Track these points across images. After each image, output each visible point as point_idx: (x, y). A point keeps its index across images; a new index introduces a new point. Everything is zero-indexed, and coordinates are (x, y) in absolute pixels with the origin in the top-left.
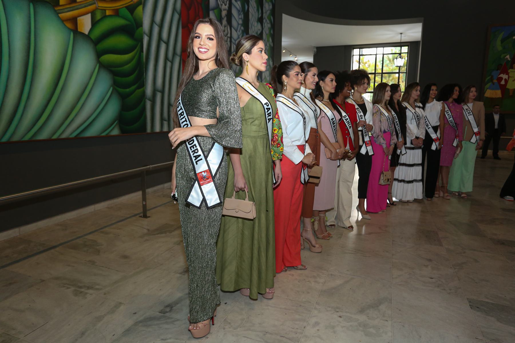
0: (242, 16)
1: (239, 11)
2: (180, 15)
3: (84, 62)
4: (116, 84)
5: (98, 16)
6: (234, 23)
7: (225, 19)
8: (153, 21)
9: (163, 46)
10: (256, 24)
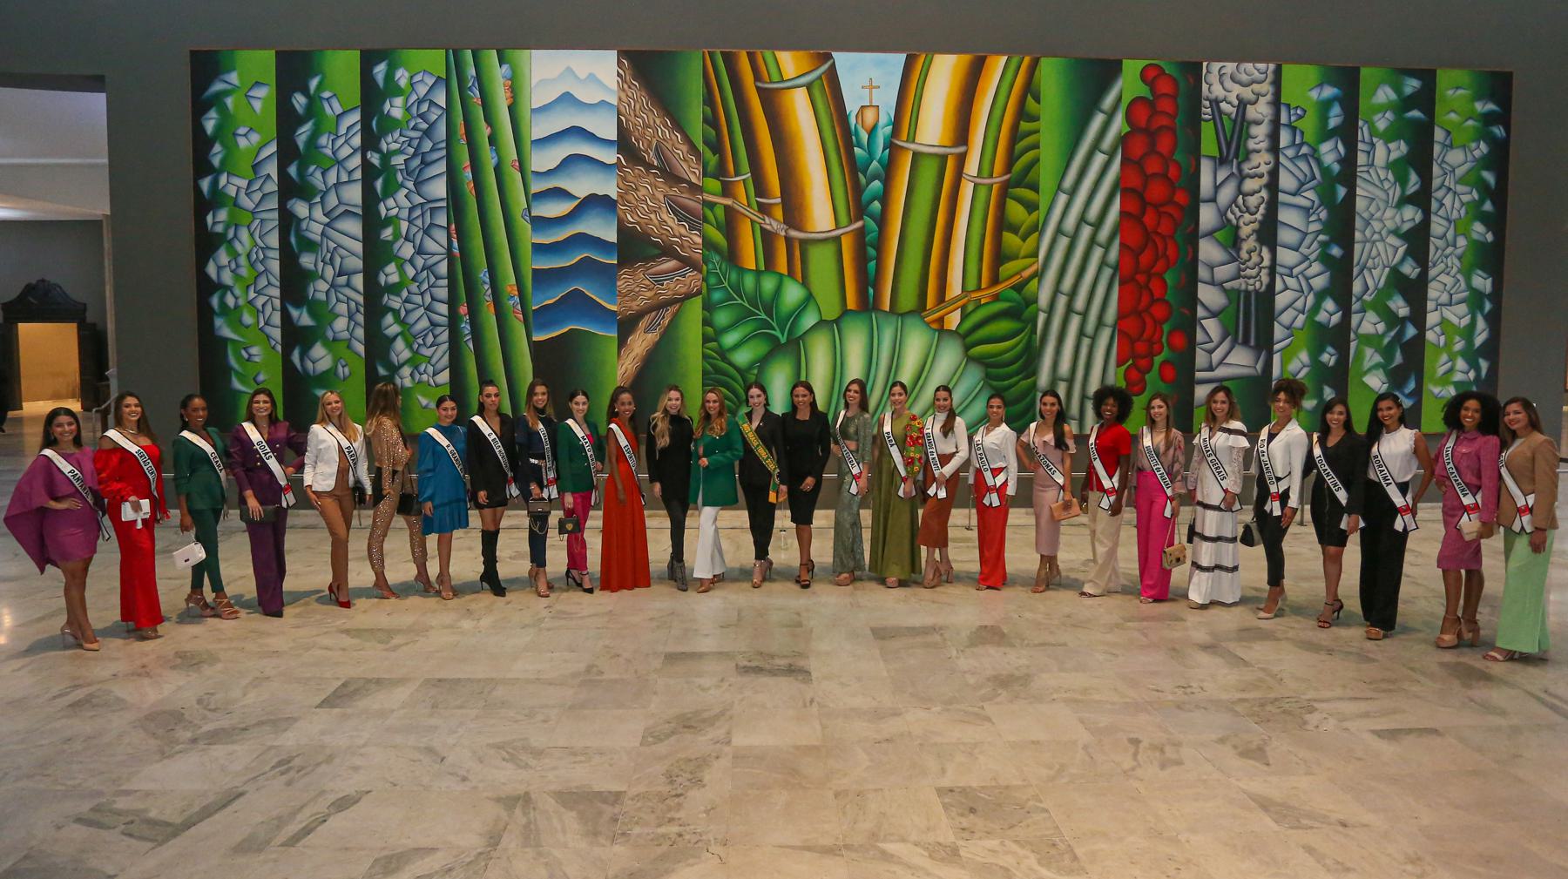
0: (1323, 215)
1: (1307, 211)
2: (1117, 268)
3: (949, 358)
4: (988, 377)
5: (970, 308)
6: (1285, 236)
7: (1253, 237)
8: (1056, 291)
9: (1075, 321)
10: (1389, 213)
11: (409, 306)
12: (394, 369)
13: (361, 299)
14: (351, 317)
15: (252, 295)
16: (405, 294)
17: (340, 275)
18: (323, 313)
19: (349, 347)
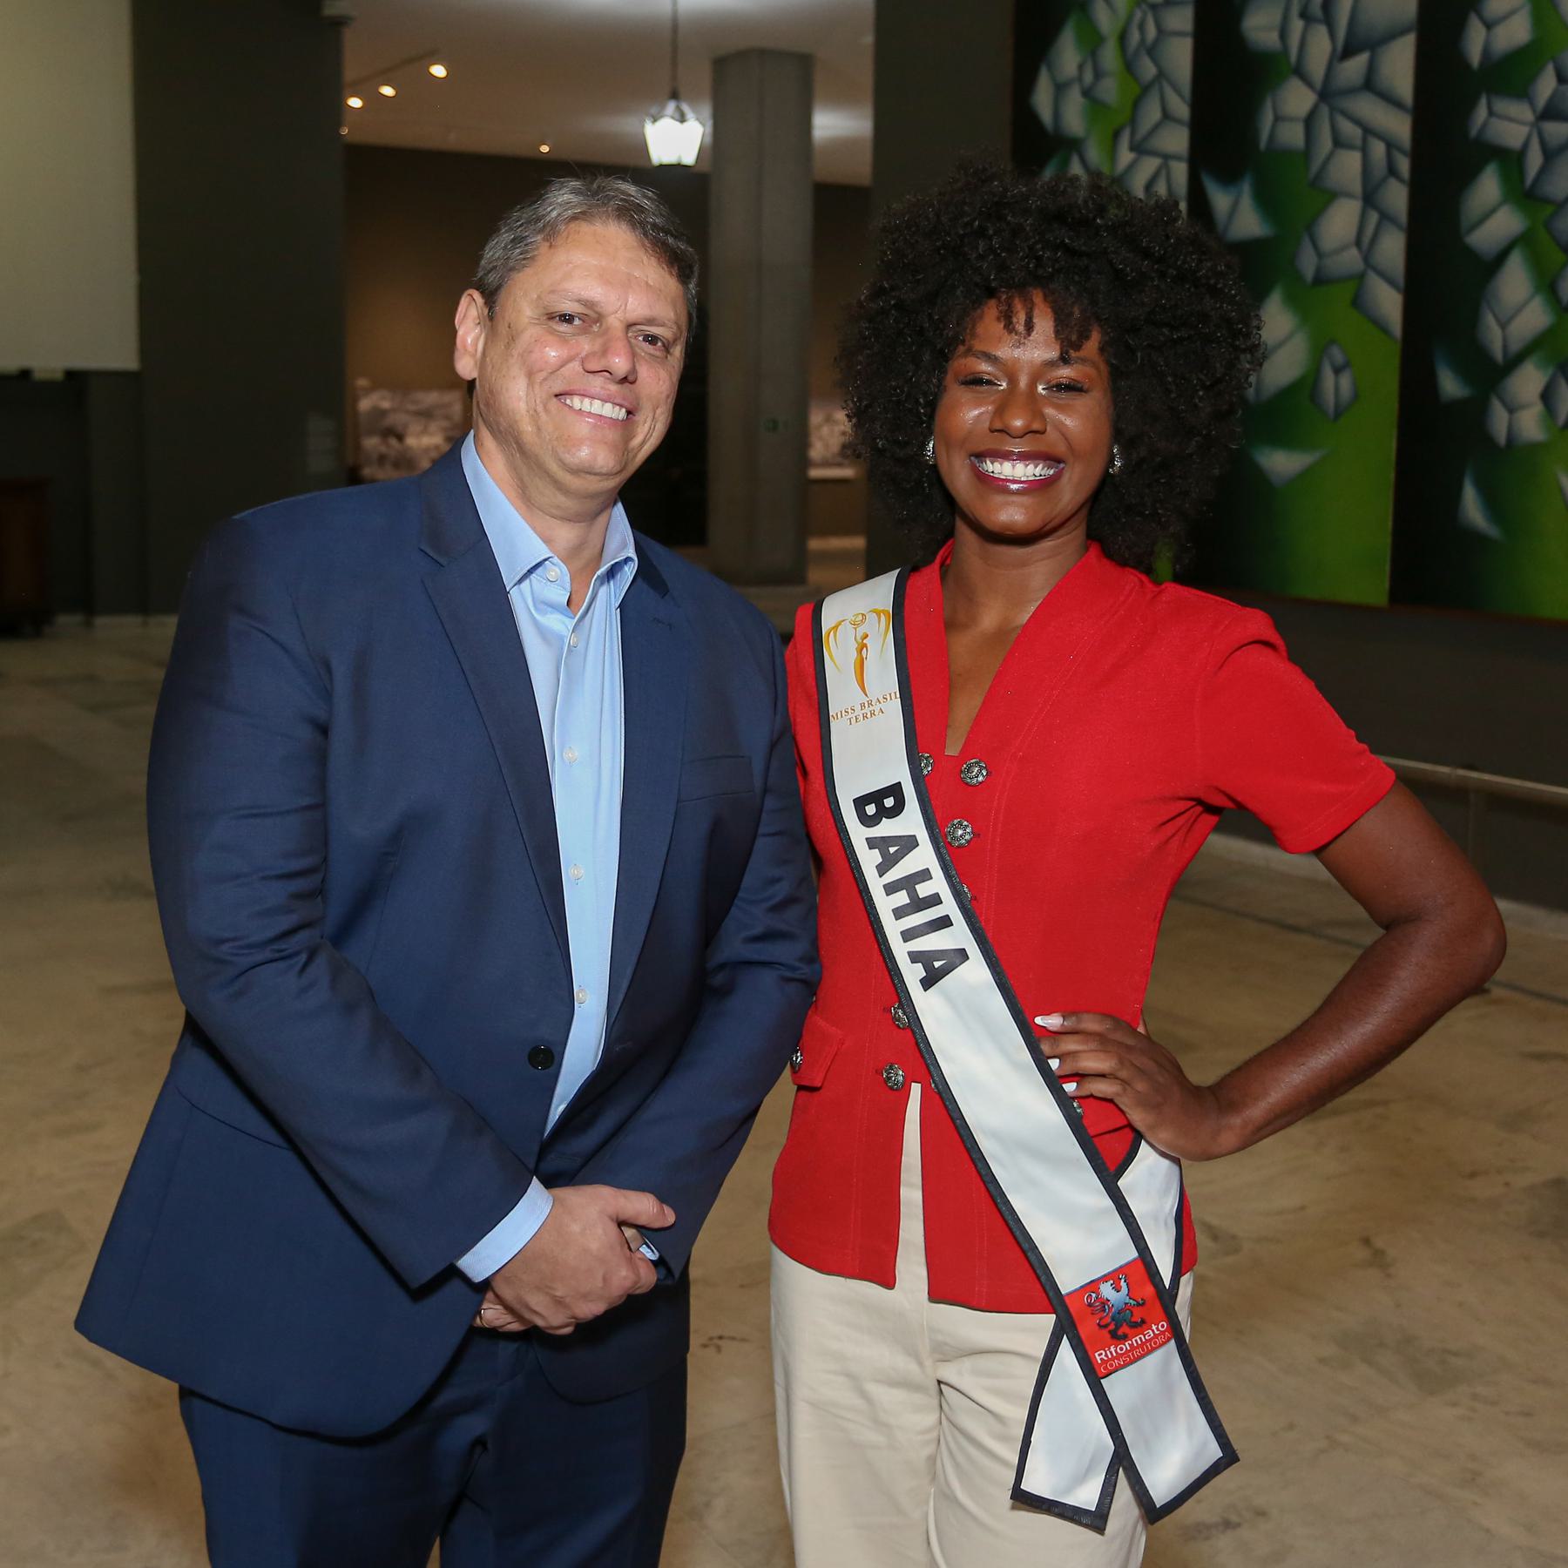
11: (1558, 131)
12: (1490, 375)
13: (1400, 127)
14: (1370, 198)
15: (1125, 156)
16: (1546, 85)
17: (1348, 52)
18: (1291, 190)
19: (1358, 301)
